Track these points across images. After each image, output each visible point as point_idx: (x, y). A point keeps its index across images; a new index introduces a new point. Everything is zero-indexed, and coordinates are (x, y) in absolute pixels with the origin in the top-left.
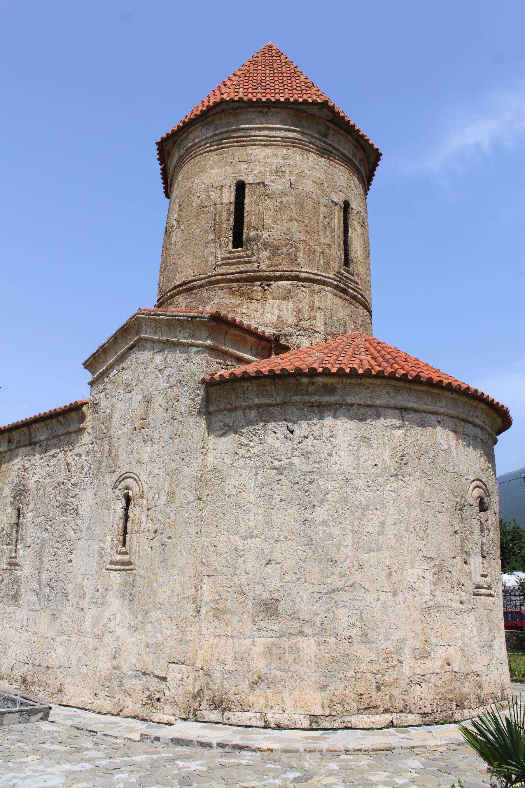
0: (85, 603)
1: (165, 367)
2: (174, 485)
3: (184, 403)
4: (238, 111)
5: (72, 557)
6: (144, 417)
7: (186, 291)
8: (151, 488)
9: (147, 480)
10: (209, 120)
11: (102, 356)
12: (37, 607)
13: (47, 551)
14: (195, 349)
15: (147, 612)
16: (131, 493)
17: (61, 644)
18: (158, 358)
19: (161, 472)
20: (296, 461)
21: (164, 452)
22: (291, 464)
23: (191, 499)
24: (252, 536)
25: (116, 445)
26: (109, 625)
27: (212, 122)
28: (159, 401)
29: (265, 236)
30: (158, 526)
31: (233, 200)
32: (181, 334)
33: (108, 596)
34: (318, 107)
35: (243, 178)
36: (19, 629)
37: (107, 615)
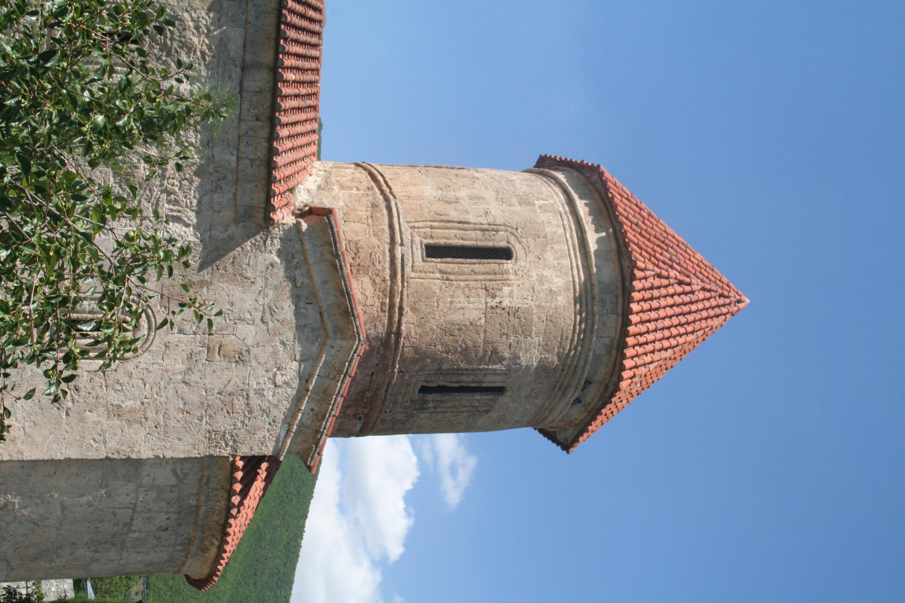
3: (223, 423)
4: (602, 388)
6: (222, 352)
8: (130, 376)
9: (143, 365)
14: (283, 434)
20: (137, 535)
22: (134, 531)
23: (109, 445)
24: (63, 508)
27: (610, 353)
29: (422, 415)
30: (83, 393)
31: (484, 385)
32: (309, 411)
34: (569, 440)
35: (508, 394)
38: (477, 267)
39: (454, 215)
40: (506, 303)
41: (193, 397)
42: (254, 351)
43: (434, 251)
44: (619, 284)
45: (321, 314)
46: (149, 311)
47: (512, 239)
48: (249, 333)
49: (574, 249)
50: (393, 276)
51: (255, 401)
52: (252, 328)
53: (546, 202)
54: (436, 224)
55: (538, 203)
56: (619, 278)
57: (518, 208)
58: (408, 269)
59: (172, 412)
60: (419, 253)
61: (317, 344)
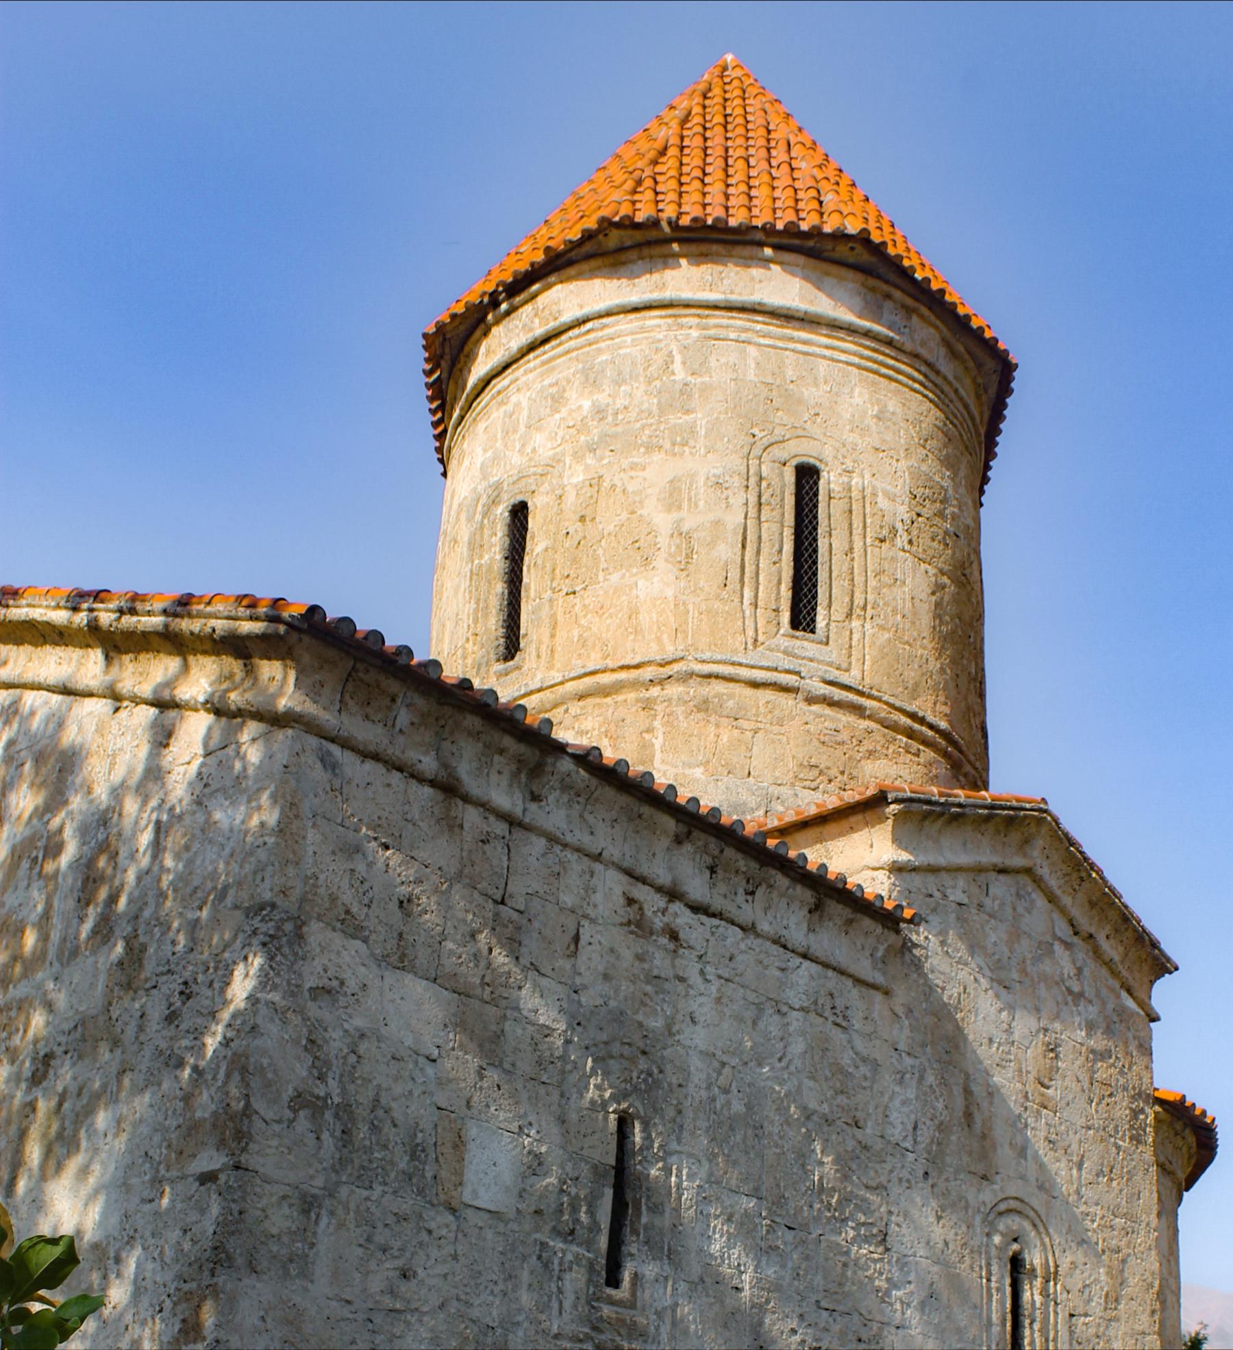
38: (839, 543)
39: (727, 551)
43: (802, 616)
45: (1002, 871)
47: (779, 453)
49: (791, 339)
50: (858, 710)
53: (678, 359)
54: (748, 594)
55: (680, 374)
57: (701, 418)
58: (845, 679)
60: (804, 645)
61: (1034, 896)
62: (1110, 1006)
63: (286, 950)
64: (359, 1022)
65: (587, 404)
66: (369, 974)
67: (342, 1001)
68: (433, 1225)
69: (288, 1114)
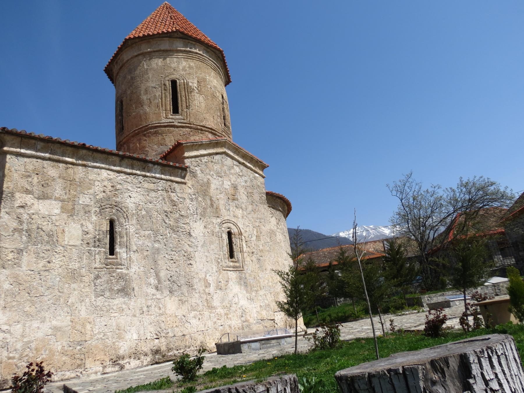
0: (212, 289)
1: (242, 175)
2: (259, 233)
3: (256, 197)
5: (191, 262)
7: (211, 133)
10: (209, 50)
11: (197, 147)
12: (158, 296)
13: (162, 256)
15: (257, 291)
16: (232, 231)
17: (195, 317)
18: (237, 169)
19: (250, 225)
21: (250, 216)
23: (269, 241)
25: (217, 202)
26: (234, 300)
28: (241, 190)
30: (254, 250)
33: (229, 285)
36: (137, 315)
37: (231, 295)
40: (196, 85)
41: (250, 208)
42: (232, 182)
43: (176, 110)
44: (184, 40)
46: (224, 222)
47: (167, 79)
48: (227, 184)
51: (248, 184)
52: (225, 182)
56: (181, 40)
58: (185, 121)
59: (255, 216)
62: (251, 177)
63: (9, 200)
64: (32, 211)
65: (130, 77)
66: (35, 201)
67: (26, 208)
68: (57, 250)
69: (12, 233)
